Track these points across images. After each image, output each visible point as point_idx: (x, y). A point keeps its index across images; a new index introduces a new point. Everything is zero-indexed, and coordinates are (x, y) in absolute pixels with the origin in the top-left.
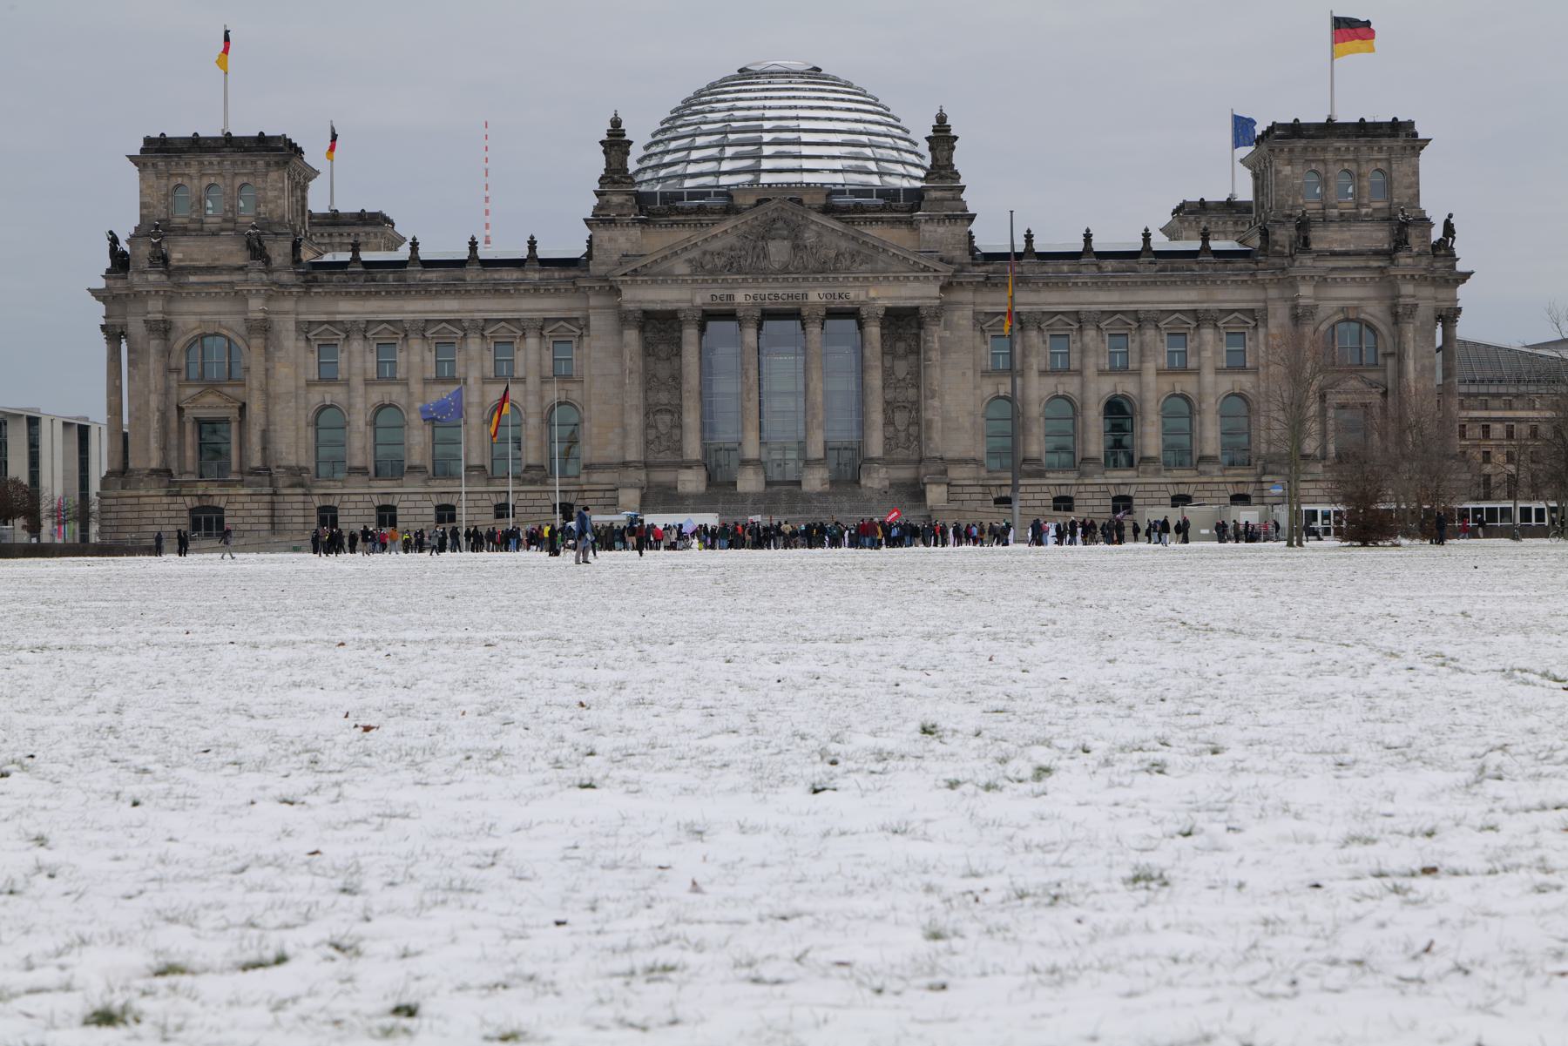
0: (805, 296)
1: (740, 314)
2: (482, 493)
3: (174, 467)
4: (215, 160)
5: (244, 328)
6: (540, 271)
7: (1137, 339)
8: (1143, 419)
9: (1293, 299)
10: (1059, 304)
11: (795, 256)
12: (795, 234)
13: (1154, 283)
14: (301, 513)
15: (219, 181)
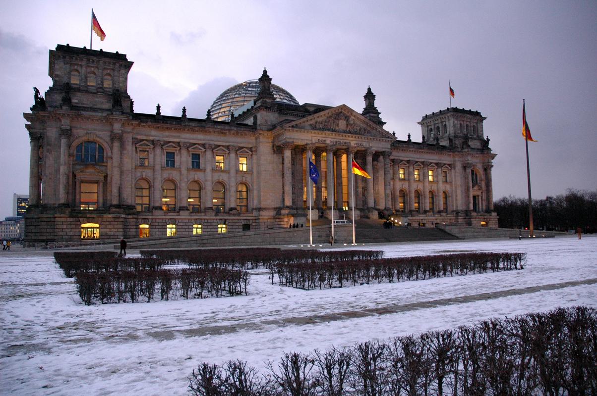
0: (350, 143)
1: (329, 148)
2: (214, 219)
3: (70, 201)
4: (95, 59)
5: (110, 139)
6: (237, 127)
7: (422, 171)
8: (425, 197)
9: (462, 161)
10: (404, 157)
11: (347, 127)
12: (347, 118)
13: (429, 153)
14: (135, 227)
15: (96, 71)
